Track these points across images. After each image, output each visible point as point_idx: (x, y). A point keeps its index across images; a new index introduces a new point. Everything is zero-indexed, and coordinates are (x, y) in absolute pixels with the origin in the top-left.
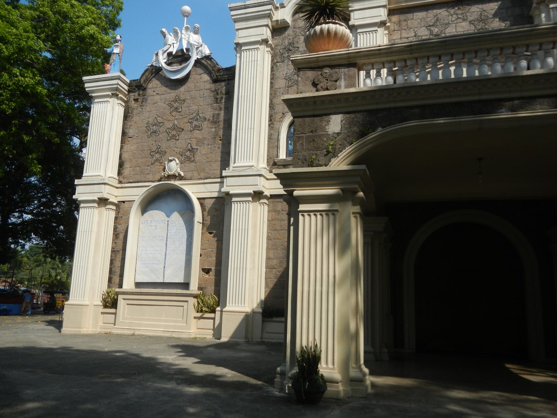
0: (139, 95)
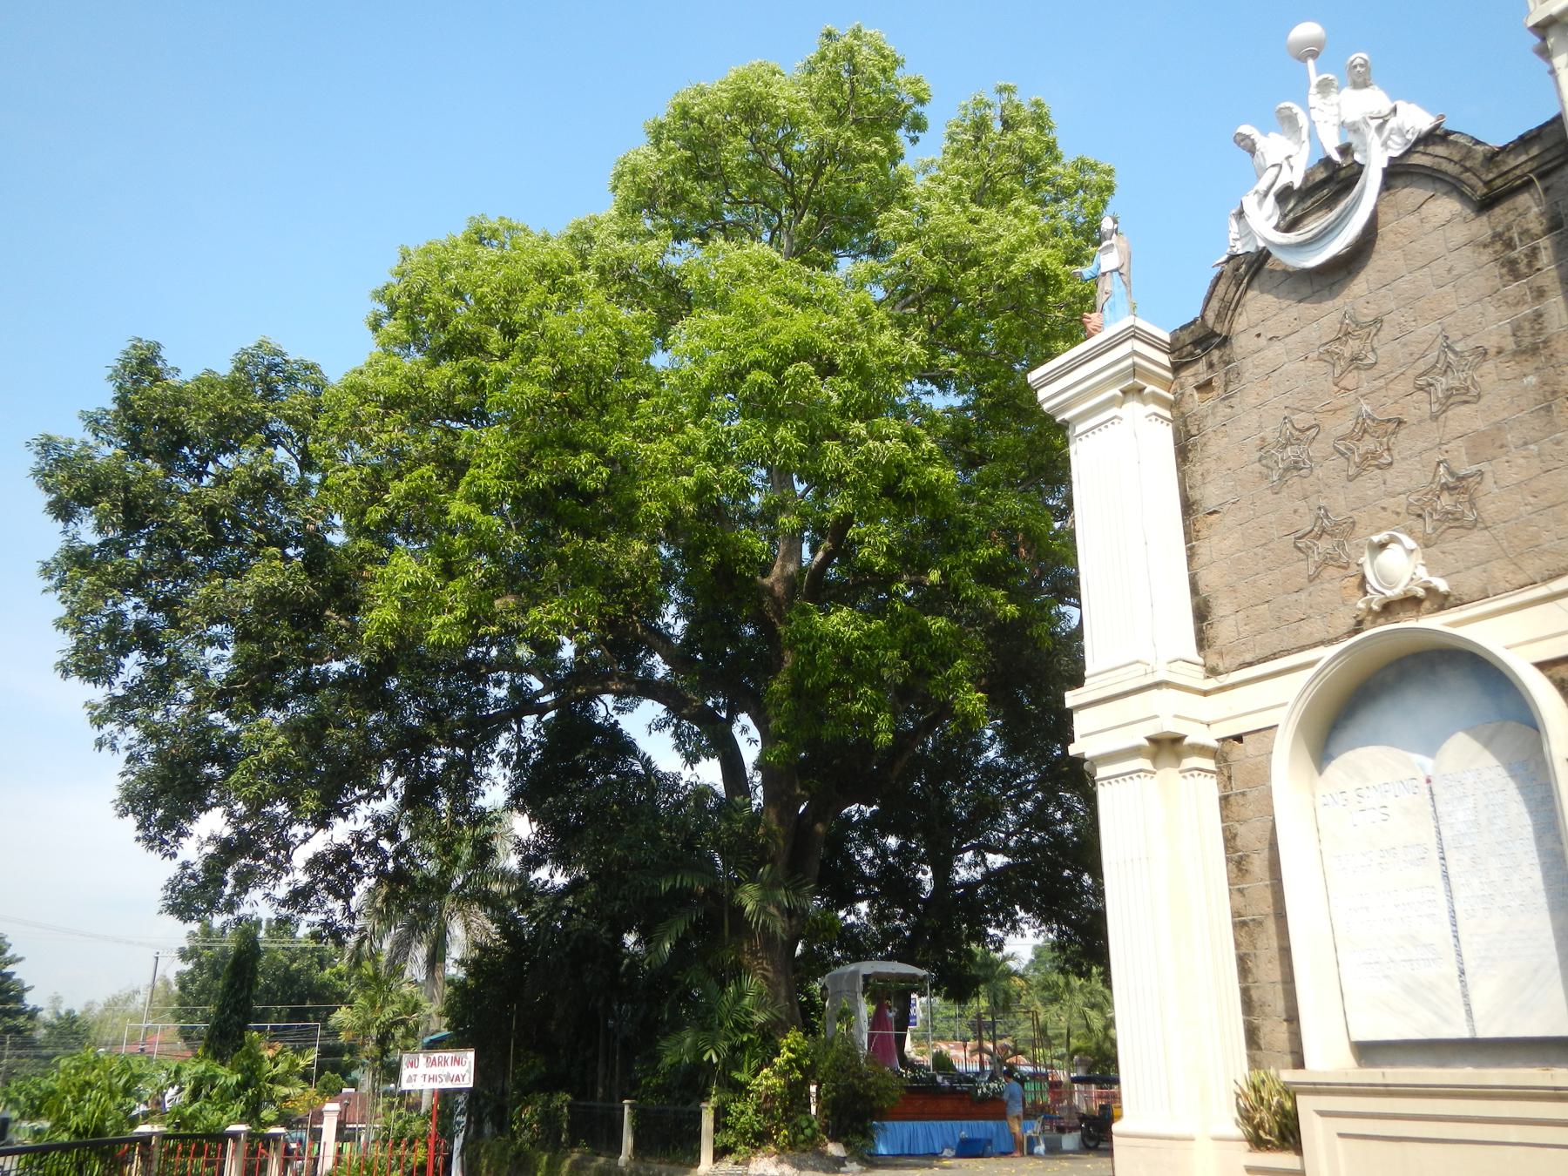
0: (1211, 366)
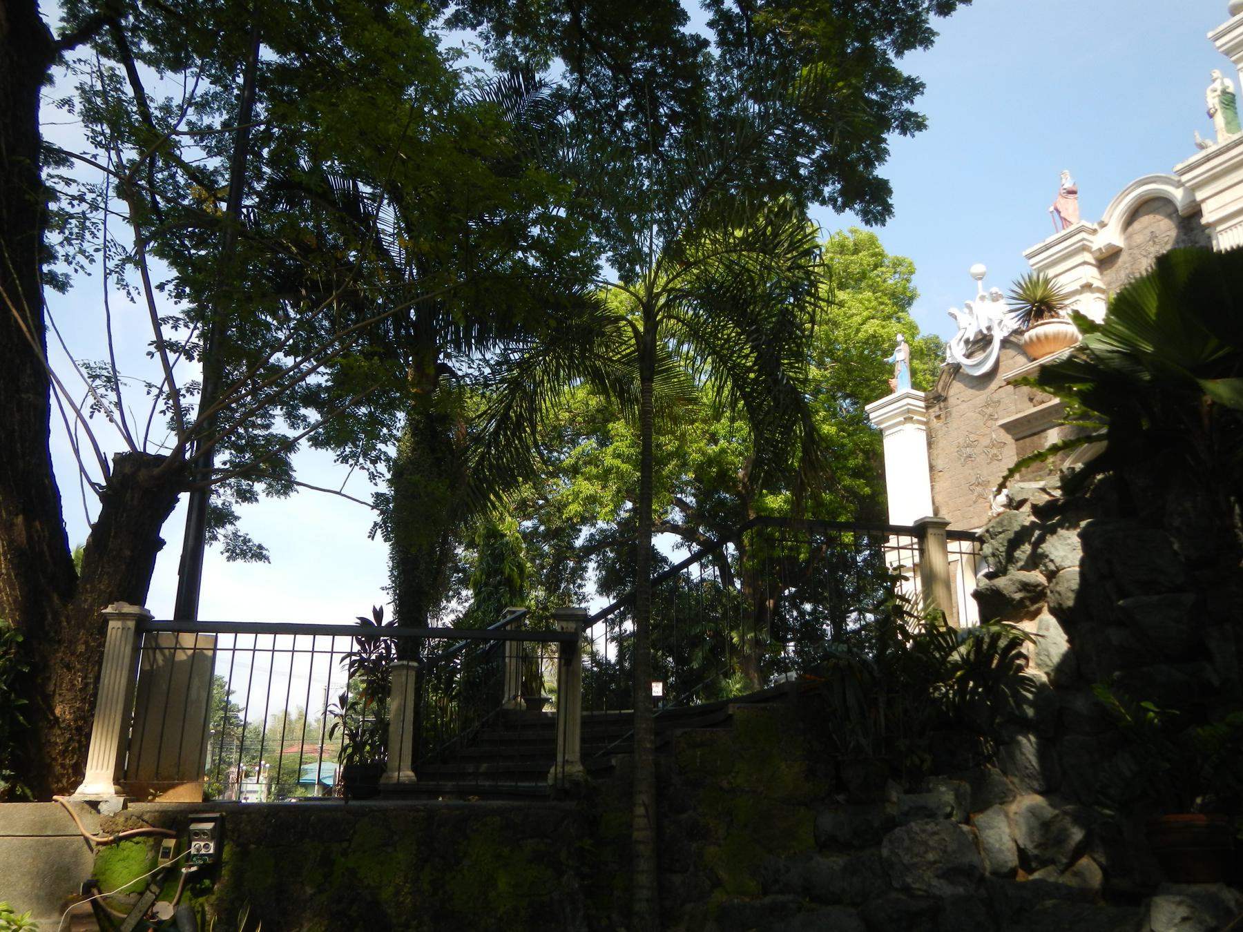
0: (940, 409)
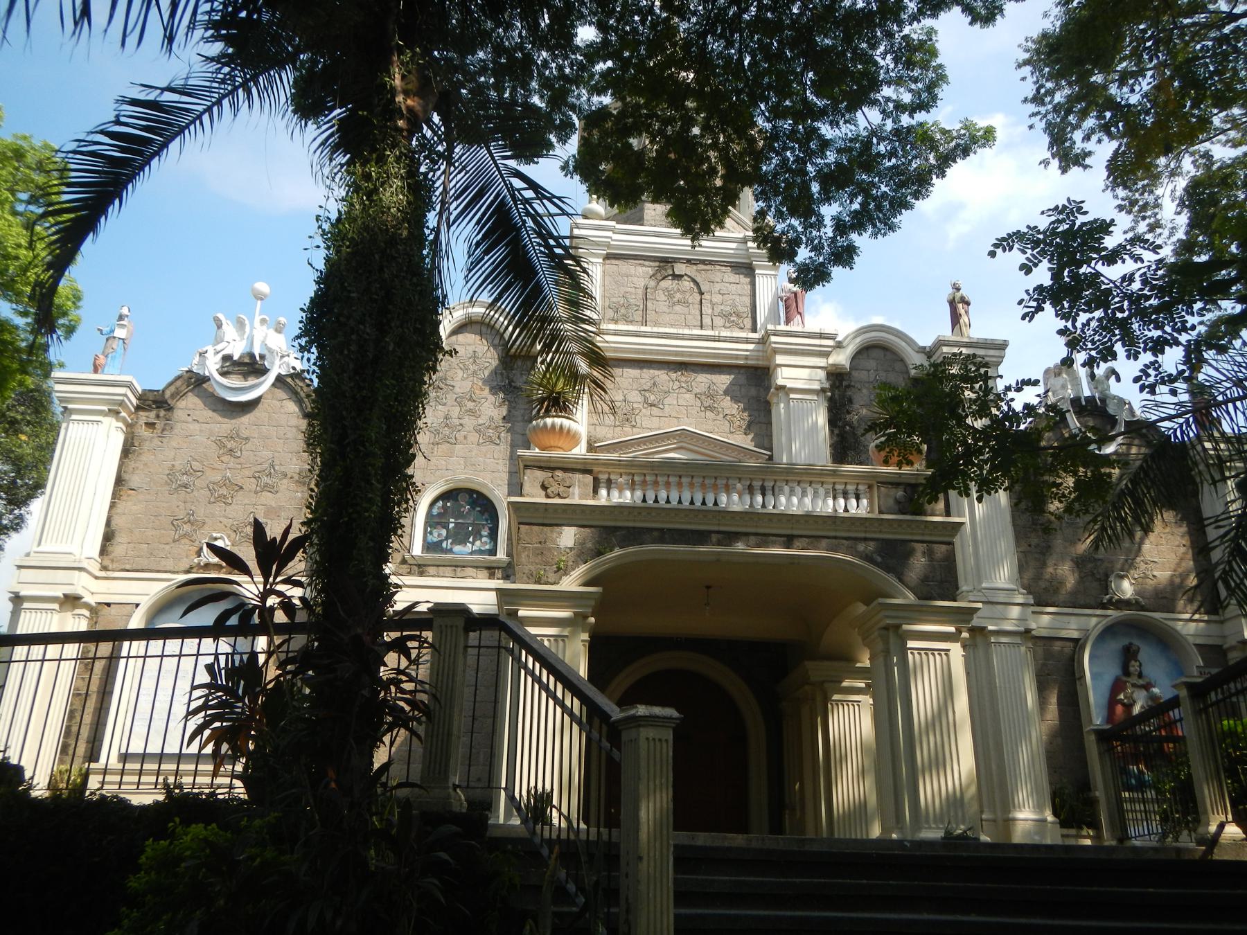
0: (158, 416)
